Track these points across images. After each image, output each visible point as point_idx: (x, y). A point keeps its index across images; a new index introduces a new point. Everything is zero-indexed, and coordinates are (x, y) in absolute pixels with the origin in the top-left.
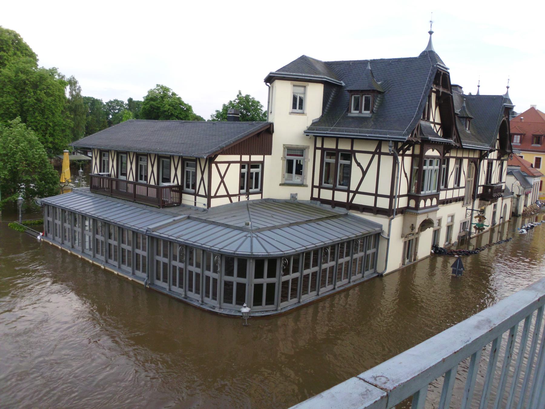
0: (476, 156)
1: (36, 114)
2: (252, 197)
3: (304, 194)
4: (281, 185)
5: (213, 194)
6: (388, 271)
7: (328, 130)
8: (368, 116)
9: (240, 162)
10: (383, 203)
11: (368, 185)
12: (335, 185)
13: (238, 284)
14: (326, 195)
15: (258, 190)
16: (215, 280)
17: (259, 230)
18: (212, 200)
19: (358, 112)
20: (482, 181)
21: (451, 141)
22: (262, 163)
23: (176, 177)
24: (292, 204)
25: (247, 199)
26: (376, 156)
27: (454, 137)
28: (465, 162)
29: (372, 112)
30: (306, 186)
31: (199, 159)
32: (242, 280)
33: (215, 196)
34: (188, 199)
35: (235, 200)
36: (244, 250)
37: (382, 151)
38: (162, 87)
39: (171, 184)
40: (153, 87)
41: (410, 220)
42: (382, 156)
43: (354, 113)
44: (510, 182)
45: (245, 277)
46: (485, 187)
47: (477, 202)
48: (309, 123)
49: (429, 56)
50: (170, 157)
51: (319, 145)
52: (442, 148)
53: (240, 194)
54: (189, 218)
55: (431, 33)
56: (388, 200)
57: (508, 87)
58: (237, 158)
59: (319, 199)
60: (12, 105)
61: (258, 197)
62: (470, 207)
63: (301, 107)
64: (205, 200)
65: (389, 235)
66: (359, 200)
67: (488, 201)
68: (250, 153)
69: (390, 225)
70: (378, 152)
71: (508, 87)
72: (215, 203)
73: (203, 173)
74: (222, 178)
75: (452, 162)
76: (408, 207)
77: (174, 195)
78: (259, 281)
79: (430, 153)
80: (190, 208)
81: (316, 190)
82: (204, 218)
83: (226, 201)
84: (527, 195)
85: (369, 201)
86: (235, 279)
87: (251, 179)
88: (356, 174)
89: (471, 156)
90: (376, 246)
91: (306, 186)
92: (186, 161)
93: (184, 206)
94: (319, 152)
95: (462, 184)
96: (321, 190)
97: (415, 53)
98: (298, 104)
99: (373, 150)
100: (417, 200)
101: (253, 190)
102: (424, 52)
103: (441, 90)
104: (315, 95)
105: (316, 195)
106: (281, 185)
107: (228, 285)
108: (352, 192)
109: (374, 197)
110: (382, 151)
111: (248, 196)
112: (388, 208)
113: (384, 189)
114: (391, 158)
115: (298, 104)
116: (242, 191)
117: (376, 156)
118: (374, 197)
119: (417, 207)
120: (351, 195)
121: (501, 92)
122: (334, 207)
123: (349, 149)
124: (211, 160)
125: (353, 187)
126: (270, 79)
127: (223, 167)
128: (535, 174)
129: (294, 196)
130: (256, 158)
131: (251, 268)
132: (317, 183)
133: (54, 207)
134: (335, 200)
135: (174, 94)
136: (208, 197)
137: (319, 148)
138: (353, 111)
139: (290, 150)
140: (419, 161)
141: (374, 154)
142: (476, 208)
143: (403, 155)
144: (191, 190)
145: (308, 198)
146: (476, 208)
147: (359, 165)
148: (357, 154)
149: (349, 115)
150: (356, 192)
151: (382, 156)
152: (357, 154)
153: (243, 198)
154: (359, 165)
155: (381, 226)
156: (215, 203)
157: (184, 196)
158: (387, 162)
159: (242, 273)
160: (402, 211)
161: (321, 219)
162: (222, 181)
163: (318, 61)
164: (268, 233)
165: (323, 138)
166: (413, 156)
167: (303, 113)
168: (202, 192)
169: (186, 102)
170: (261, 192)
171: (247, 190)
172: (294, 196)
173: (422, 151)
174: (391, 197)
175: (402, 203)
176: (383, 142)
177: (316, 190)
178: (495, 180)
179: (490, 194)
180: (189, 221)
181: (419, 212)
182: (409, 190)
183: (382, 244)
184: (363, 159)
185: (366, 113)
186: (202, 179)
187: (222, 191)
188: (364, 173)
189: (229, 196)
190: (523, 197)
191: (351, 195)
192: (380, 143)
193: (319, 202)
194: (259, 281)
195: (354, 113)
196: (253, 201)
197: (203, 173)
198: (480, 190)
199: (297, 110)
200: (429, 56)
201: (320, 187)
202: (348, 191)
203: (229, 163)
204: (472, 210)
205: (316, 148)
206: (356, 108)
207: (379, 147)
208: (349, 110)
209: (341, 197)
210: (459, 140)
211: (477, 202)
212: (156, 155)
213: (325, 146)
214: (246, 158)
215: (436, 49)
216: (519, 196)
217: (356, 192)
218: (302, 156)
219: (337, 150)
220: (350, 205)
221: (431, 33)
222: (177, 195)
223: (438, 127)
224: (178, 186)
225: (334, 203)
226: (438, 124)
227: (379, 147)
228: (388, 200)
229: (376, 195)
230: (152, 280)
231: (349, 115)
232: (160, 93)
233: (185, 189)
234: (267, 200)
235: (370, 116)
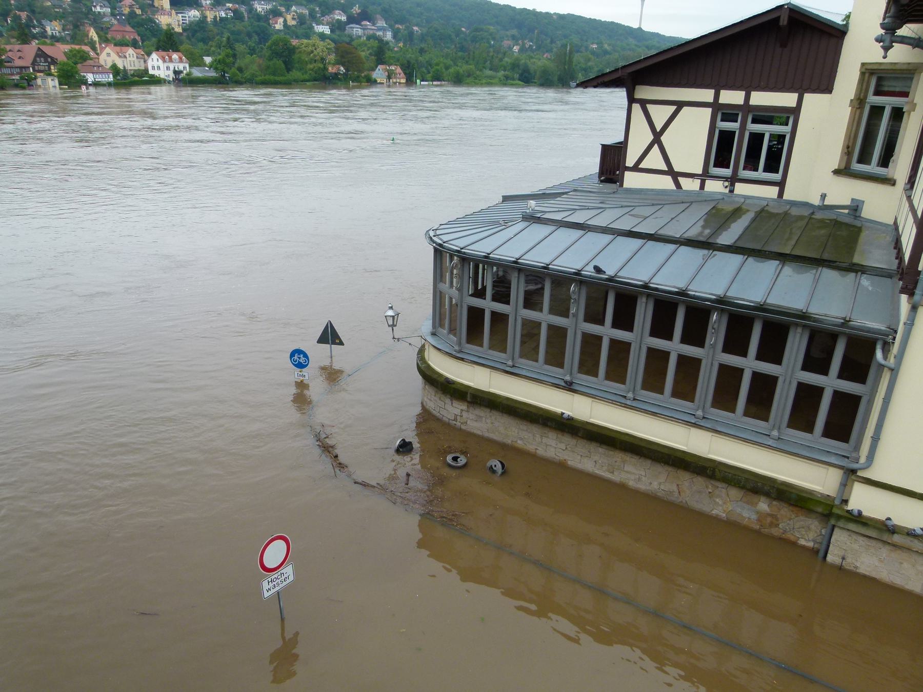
2: (741, 189)
4: (837, 172)
15: (777, 177)
22: (795, 111)
25: (727, 191)
32: (621, 335)
33: (636, 168)
53: (705, 175)
101: (760, 174)
106: (837, 172)
111: (733, 185)
127: (660, 114)
130: (760, 98)
153: (715, 187)
196: (746, 197)
203: (680, 105)
214: (732, 97)
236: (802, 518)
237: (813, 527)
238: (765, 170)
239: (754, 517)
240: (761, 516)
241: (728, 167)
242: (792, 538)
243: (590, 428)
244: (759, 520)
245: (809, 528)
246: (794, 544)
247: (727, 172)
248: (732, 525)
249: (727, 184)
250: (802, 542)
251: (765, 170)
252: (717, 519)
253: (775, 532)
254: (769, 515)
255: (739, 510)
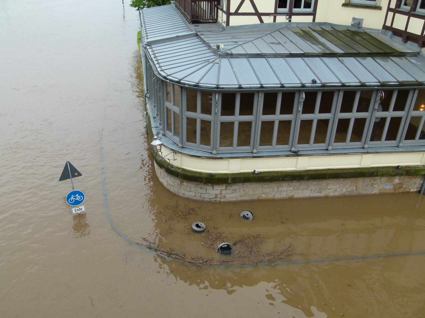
2: (295, 19)
4: (344, 5)
5: (232, 10)
14: (400, 21)
15: (310, 10)
18: (231, 17)
25: (287, 21)
33: (236, 13)
35: (268, 20)
53: (275, 14)
61: (309, 19)
83: (255, 20)
105: (388, 24)
111: (290, 17)
116: (280, 10)
122: (406, 42)
129: (358, 23)
132: (393, 6)
134: (408, 30)
145: (380, 27)
170: (314, 14)
171: (290, 10)
172: (358, 23)
187: (247, 7)
193: (390, 33)
196: (297, 23)
201: (395, 11)
236: (413, 179)
237: (417, 182)
238: (304, 7)
239: (392, 187)
240: (395, 186)
241: (285, 7)
242: (408, 190)
243: (310, 173)
244: (394, 188)
245: (416, 183)
246: (408, 192)
247: (286, 10)
248: (382, 195)
249: (288, 17)
250: (412, 190)
251: (304, 7)
252: (375, 195)
253: (401, 190)
254: (399, 184)
255: (385, 187)
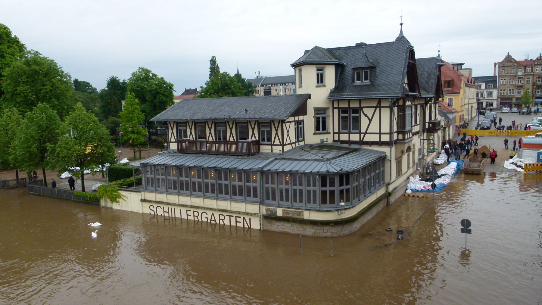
0: (423, 102)
1: (53, 99)
3: (329, 139)
4: (314, 134)
6: (392, 181)
7: (344, 95)
8: (368, 84)
9: (295, 121)
10: (385, 138)
11: (375, 127)
12: (350, 131)
13: (330, 191)
14: (344, 137)
16: (315, 192)
17: (328, 160)
19: (360, 82)
20: (427, 120)
21: (416, 94)
22: (303, 121)
23: (253, 135)
24: (323, 146)
26: (378, 109)
27: (417, 91)
28: (419, 106)
29: (371, 81)
30: (330, 133)
31: (273, 121)
33: (286, 145)
34: (265, 149)
35: (294, 146)
36: (332, 170)
37: (382, 105)
38: (143, 70)
39: (250, 140)
40: (136, 70)
41: (400, 147)
42: (382, 109)
43: (358, 83)
44: (439, 118)
45: (334, 186)
46: (429, 123)
47: (425, 134)
48: (329, 92)
49: (401, 39)
50: (248, 122)
51: (336, 105)
52: (412, 99)
53: (296, 142)
54: (276, 159)
55: (401, 24)
56: (389, 135)
57: (439, 51)
58: (292, 119)
59: (339, 141)
60: (29, 92)
62: (422, 138)
63: (322, 82)
64: (280, 148)
65: (391, 158)
66: (368, 138)
67: (433, 132)
68: (298, 115)
69: (391, 151)
70: (379, 106)
71: (439, 51)
72: (287, 148)
73: (277, 130)
74: (288, 132)
75: (413, 107)
76: (398, 139)
77: (254, 148)
78: (342, 188)
79: (408, 103)
80: (267, 154)
81: (336, 136)
82: (288, 157)
84: (449, 128)
85: (376, 138)
86: (328, 189)
87: (300, 133)
88: (364, 122)
89: (421, 103)
90: (383, 166)
91: (330, 133)
92: (260, 123)
93: (262, 153)
94: (336, 111)
95: (418, 123)
96: (340, 135)
97: (393, 40)
98: (320, 79)
99: (375, 105)
100: (404, 133)
102: (398, 38)
103: (411, 62)
104: (330, 73)
105: (336, 138)
106: (314, 134)
107: (324, 193)
108: (363, 133)
109: (378, 135)
110: (382, 105)
112: (388, 140)
113: (386, 128)
114: (388, 109)
115: (320, 79)
117: (378, 109)
118: (378, 135)
119: (404, 139)
120: (362, 135)
121: (435, 55)
123: (358, 106)
124: (283, 122)
125: (363, 130)
126: (296, 65)
128: (453, 111)
129: (322, 141)
130: (301, 118)
131: (337, 181)
132: (336, 130)
133: (155, 166)
135: (155, 75)
136: (283, 145)
137: (336, 108)
138: (356, 82)
139: (317, 110)
140: (402, 109)
141: (376, 107)
142: (425, 138)
143: (395, 106)
144: (266, 142)
146: (425, 138)
147: (366, 115)
148: (364, 109)
149: (354, 84)
150: (366, 133)
151: (382, 109)
152: (364, 109)
153: (297, 145)
154: (366, 115)
155: (385, 153)
156: (287, 148)
157: (261, 147)
158: (386, 113)
159: (332, 184)
160: (396, 142)
161: (346, 154)
162: (288, 135)
163: (324, 49)
164: (332, 161)
165: (338, 101)
166: (398, 106)
167: (324, 86)
168: (277, 142)
169: (168, 82)
170: (303, 140)
171: (298, 139)
172: (322, 141)
173: (404, 103)
174: (391, 133)
175: (395, 136)
176: (382, 100)
177: (336, 136)
178: (433, 119)
179: (433, 127)
180: (277, 161)
181: (406, 141)
182: (398, 129)
183: (387, 165)
184: (369, 112)
185: (367, 82)
186: (277, 134)
188: (370, 121)
189: (291, 144)
190: (447, 129)
191: (362, 135)
192: (380, 100)
194: (342, 188)
195: (358, 83)
197: (277, 130)
198: (427, 126)
199: (320, 84)
200: (401, 39)
201: (339, 133)
202: (360, 133)
204: (423, 139)
205: (334, 108)
206: (359, 79)
207: (379, 103)
208: (353, 81)
209: (355, 137)
210: (420, 93)
211: (425, 134)
212: (256, 121)
213: (340, 106)
214: (296, 118)
215: (405, 35)
216: (445, 128)
217: (366, 133)
218: (325, 114)
219: (349, 108)
220: (362, 142)
221: (401, 24)
222: (257, 146)
223: (407, 85)
224: (256, 141)
225: (350, 142)
226: (406, 84)
227: (379, 103)
228: (389, 135)
229: (380, 133)
230: (263, 201)
231: (354, 84)
232: (141, 75)
233: (261, 142)
234: (307, 145)
235: (369, 83)
